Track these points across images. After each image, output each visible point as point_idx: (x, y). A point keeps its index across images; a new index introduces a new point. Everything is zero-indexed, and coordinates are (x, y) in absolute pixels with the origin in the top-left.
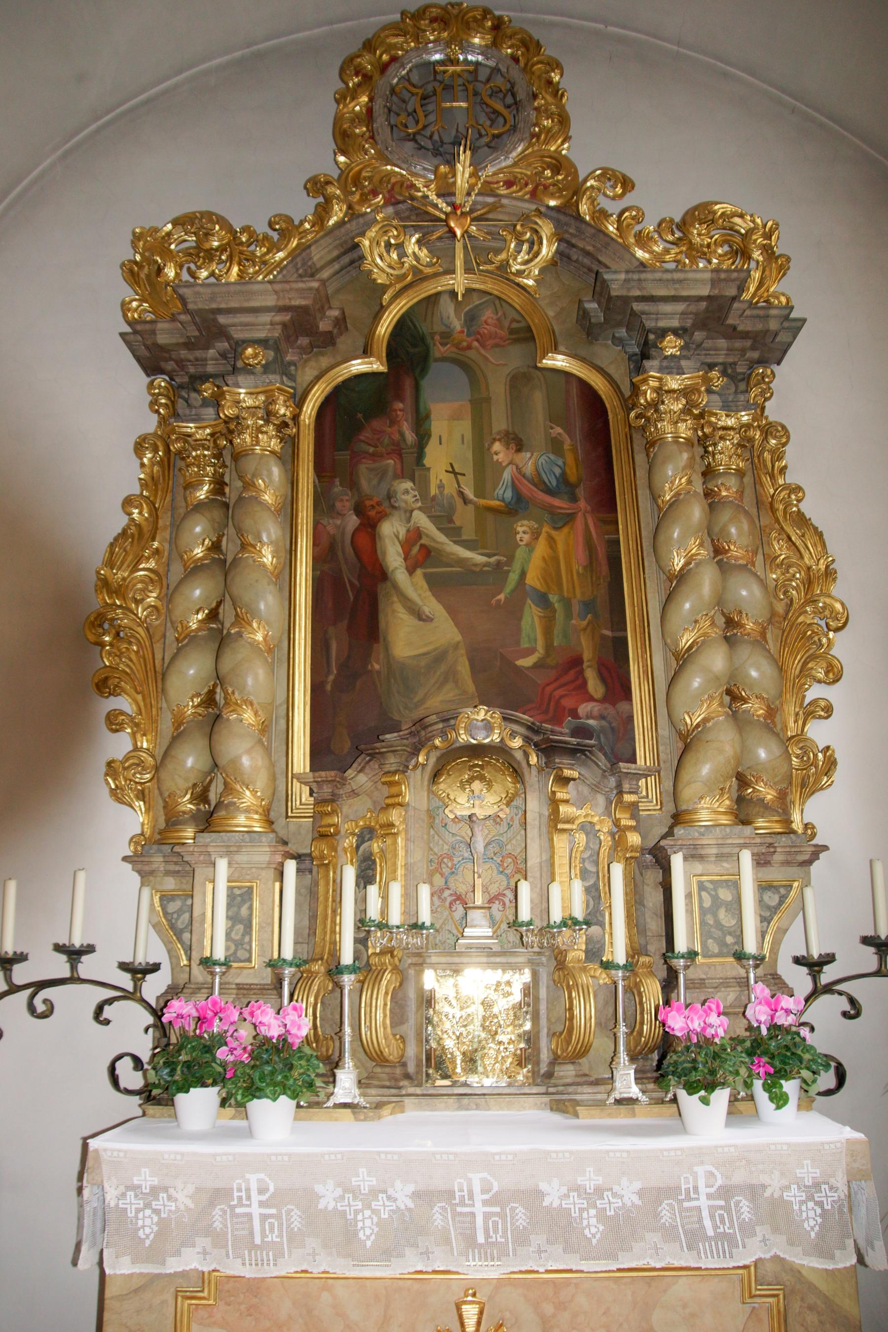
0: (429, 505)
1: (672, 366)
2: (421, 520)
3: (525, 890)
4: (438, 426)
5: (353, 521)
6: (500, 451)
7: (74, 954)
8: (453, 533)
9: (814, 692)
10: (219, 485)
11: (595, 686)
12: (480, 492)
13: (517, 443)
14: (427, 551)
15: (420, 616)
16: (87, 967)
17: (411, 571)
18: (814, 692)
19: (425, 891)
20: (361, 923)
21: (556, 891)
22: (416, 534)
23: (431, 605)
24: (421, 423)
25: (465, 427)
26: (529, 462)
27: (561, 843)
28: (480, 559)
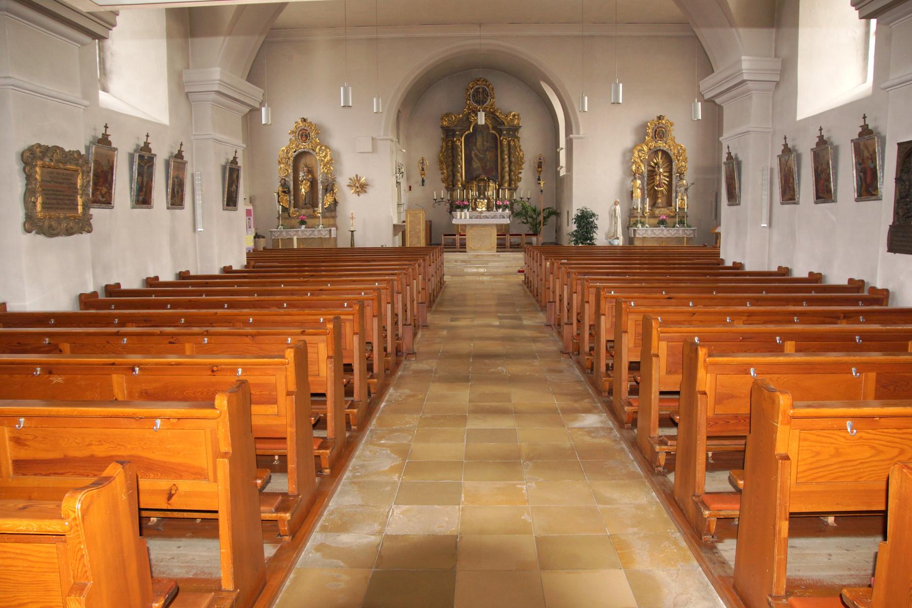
0: (477, 150)
1: (504, 135)
2: (476, 151)
3: (486, 192)
4: (478, 140)
5: (468, 152)
6: (485, 143)
7: (442, 199)
8: (479, 153)
9: (520, 171)
10: (452, 146)
11: (495, 171)
12: (483, 148)
13: (487, 142)
14: (477, 155)
15: (475, 162)
16: (443, 200)
17: (475, 157)
18: (520, 171)
19: (477, 193)
20: (472, 195)
21: (489, 193)
22: (476, 153)
23: (477, 161)
24: (476, 139)
25: (481, 140)
26: (488, 145)
27: (490, 188)
28: (482, 156)
